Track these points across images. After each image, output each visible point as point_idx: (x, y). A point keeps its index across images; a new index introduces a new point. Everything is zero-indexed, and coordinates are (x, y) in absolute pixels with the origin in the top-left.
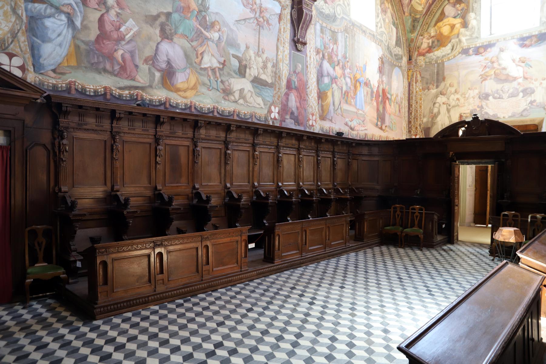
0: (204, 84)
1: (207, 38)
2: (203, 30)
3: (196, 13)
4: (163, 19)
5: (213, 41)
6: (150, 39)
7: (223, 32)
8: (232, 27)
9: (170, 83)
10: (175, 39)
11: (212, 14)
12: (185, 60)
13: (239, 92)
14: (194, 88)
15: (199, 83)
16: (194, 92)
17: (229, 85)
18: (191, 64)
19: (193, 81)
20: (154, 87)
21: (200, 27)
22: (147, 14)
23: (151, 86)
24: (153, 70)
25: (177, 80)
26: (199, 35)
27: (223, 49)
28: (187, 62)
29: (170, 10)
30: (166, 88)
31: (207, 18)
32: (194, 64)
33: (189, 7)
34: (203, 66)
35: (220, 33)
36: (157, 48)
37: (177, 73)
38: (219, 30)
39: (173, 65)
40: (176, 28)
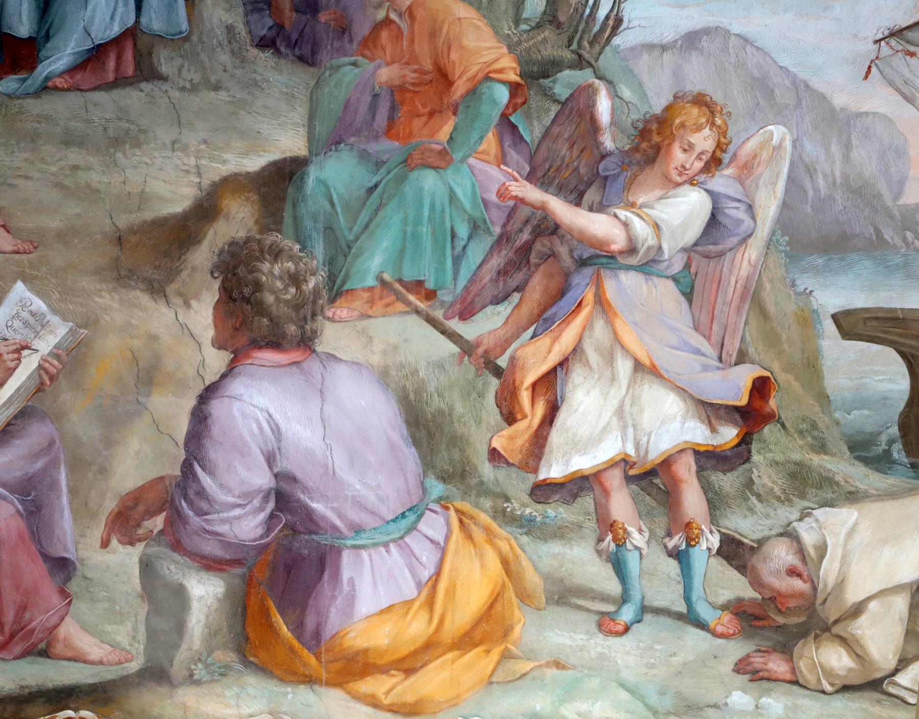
0: (564, 594)
1: (598, 258)
2: (560, 209)
3: (502, 94)
4: (238, 220)
5: (649, 266)
6: (148, 375)
7: (747, 168)
8: (839, 100)
9: (298, 628)
10: (336, 335)
11: (643, 64)
12: (410, 456)
13: (901, 604)
14: (488, 629)
15: (524, 596)
16: (479, 662)
17: (806, 563)
18: (458, 475)
19: (474, 581)
20: (177, 668)
21: (533, 193)
22: (123, 221)
23: (156, 674)
24: (173, 568)
25: (352, 599)
26: (526, 249)
27: (753, 296)
28: (427, 465)
29: (290, 142)
30: (263, 670)
31: (604, 106)
32: (487, 470)
33: (443, 77)
34: (554, 469)
35: (722, 182)
36: (200, 418)
37: (347, 558)
38: (714, 163)
39: (317, 506)
40: (340, 253)
